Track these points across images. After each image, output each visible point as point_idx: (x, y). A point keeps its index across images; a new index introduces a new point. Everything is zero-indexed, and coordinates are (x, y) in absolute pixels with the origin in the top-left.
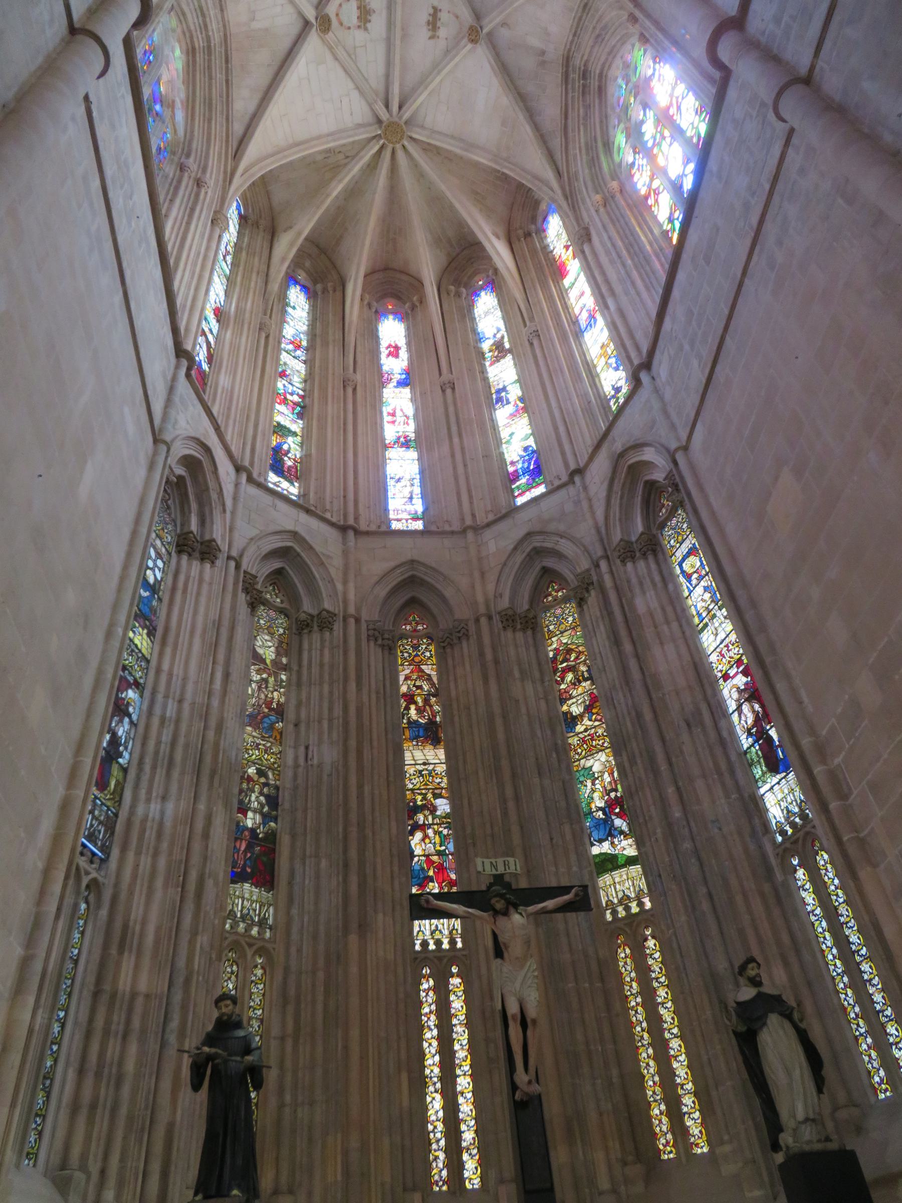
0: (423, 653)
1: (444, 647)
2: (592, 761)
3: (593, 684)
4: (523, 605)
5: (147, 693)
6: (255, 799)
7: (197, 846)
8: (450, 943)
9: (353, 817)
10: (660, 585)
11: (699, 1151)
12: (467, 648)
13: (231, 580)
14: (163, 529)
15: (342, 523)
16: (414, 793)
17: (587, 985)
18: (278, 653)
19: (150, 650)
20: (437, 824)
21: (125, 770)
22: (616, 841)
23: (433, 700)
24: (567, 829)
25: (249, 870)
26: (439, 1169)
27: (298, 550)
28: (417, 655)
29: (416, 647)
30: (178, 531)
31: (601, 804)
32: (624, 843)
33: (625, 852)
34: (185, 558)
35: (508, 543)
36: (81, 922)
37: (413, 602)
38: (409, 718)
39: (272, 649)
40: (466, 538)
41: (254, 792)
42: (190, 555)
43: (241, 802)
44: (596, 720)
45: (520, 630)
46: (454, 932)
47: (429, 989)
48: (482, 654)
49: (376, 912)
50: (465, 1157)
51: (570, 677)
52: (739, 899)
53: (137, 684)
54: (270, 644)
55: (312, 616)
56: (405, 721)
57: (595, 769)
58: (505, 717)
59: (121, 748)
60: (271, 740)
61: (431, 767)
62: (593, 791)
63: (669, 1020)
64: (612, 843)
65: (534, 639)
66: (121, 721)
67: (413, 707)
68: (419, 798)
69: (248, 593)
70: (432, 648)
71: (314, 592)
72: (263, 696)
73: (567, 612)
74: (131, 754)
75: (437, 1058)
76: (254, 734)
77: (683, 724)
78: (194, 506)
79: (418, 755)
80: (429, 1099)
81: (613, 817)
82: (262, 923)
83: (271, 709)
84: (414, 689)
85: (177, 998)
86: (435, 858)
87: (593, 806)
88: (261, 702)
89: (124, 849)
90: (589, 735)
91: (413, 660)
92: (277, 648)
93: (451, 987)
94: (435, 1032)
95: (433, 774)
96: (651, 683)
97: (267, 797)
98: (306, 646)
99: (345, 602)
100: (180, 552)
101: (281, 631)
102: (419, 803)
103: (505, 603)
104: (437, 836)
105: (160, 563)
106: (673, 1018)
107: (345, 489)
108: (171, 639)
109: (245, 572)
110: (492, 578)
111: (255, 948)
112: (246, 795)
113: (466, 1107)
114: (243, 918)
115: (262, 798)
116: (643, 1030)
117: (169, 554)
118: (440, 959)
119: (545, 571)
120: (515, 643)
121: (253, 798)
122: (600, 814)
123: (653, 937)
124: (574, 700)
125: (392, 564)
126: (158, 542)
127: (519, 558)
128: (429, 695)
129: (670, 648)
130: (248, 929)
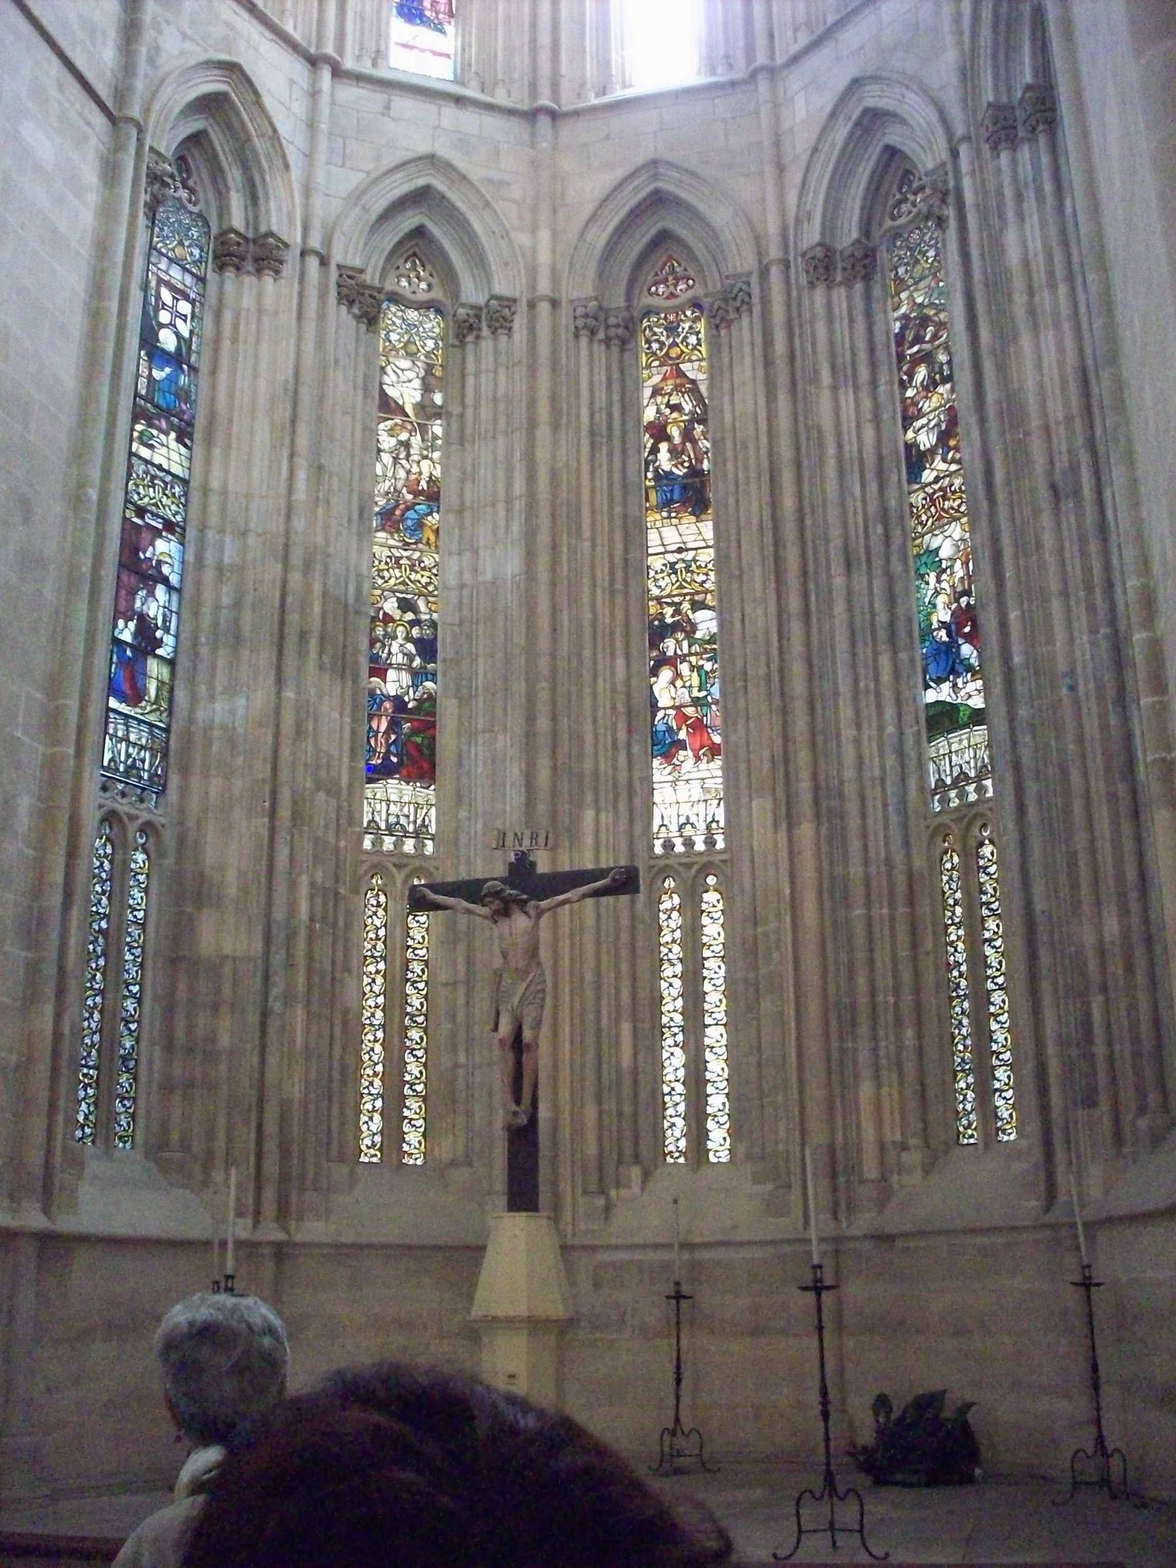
0: (686, 337)
1: (717, 327)
2: (941, 537)
3: (952, 390)
4: (849, 233)
5: (191, 534)
6: (398, 649)
7: (285, 752)
8: (705, 842)
9: (544, 663)
10: (1050, 200)
11: (1006, 1138)
12: (746, 329)
13: (312, 293)
14: (181, 243)
15: (525, 106)
16: (660, 604)
17: (885, 911)
18: (427, 389)
19: (186, 463)
20: (696, 654)
21: (171, 663)
22: (960, 681)
23: (699, 429)
24: (885, 662)
25: (395, 760)
26: (676, 1137)
27: (440, 185)
28: (675, 344)
29: (672, 329)
30: (214, 231)
31: (946, 617)
32: (971, 687)
33: (971, 703)
34: (230, 274)
35: (825, 101)
36: (142, 878)
37: (662, 238)
38: (656, 470)
39: (417, 383)
40: (756, 90)
41: (395, 638)
42: (238, 268)
43: (375, 658)
44: (953, 461)
45: (841, 283)
46: (714, 825)
47: (673, 909)
48: (768, 342)
49: (580, 805)
50: (710, 1125)
51: (921, 373)
52: (1078, 807)
53: (169, 526)
54: (411, 375)
55: (481, 309)
56: (650, 475)
57: (944, 553)
58: (798, 464)
59: (159, 634)
60: (420, 546)
61: (689, 556)
62: (937, 593)
63: (995, 964)
64: (955, 685)
65: (868, 297)
66: (151, 593)
67: (664, 447)
68: (669, 611)
69: (351, 303)
70: (701, 326)
71: (478, 259)
72: (402, 474)
73: (927, 238)
74: (176, 636)
75: (680, 1003)
76: (391, 542)
77: (1044, 493)
78: (234, 175)
79: (671, 536)
80: (665, 1055)
81: (961, 641)
82: (419, 834)
83: (416, 493)
84: (668, 411)
85: (278, 959)
86: (690, 711)
87: (934, 619)
88: (400, 484)
89: (185, 772)
90: (940, 489)
91: (667, 354)
92: (423, 379)
93: (704, 906)
94: (678, 969)
95: (694, 567)
96: (1013, 412)
97: (417, 642)
98: (470, 367)
99: (533, 272)
100: (221, 268)
101: (430, 344)
102: (669, 620)
103: (812, 234)
104: (695, 674)
105: (184, 307)
106: (1000, 963)
107: (534, 25)
108: (219, 435)
109: (339, 267)
110: (795, 177)
111: (407, 870)
112: (384, 646)
113: (716, 1066)
114: (390, 830)
115: (411, 647)
116: (961, 975)
117: (201, 280)
118: (688, 866)
119: (892, 152)
120: (832, 311)
121: (395, 648)
122: (943, 635)
123: (992, 842)
124: (924, 421)
125: (620, 173)
126: (176, 273)
127: (841, 133)
128: (691, 421)
129: (1048, 338)
130: (398, 844)
